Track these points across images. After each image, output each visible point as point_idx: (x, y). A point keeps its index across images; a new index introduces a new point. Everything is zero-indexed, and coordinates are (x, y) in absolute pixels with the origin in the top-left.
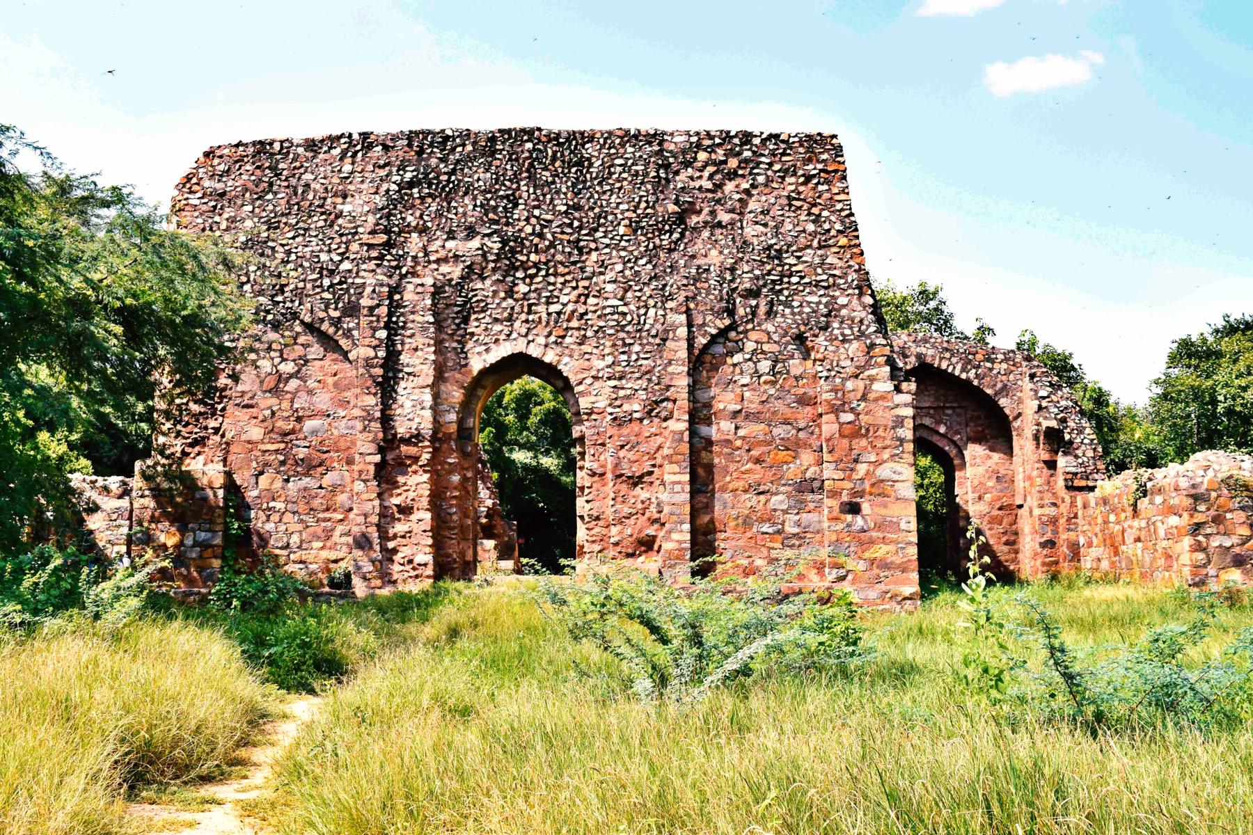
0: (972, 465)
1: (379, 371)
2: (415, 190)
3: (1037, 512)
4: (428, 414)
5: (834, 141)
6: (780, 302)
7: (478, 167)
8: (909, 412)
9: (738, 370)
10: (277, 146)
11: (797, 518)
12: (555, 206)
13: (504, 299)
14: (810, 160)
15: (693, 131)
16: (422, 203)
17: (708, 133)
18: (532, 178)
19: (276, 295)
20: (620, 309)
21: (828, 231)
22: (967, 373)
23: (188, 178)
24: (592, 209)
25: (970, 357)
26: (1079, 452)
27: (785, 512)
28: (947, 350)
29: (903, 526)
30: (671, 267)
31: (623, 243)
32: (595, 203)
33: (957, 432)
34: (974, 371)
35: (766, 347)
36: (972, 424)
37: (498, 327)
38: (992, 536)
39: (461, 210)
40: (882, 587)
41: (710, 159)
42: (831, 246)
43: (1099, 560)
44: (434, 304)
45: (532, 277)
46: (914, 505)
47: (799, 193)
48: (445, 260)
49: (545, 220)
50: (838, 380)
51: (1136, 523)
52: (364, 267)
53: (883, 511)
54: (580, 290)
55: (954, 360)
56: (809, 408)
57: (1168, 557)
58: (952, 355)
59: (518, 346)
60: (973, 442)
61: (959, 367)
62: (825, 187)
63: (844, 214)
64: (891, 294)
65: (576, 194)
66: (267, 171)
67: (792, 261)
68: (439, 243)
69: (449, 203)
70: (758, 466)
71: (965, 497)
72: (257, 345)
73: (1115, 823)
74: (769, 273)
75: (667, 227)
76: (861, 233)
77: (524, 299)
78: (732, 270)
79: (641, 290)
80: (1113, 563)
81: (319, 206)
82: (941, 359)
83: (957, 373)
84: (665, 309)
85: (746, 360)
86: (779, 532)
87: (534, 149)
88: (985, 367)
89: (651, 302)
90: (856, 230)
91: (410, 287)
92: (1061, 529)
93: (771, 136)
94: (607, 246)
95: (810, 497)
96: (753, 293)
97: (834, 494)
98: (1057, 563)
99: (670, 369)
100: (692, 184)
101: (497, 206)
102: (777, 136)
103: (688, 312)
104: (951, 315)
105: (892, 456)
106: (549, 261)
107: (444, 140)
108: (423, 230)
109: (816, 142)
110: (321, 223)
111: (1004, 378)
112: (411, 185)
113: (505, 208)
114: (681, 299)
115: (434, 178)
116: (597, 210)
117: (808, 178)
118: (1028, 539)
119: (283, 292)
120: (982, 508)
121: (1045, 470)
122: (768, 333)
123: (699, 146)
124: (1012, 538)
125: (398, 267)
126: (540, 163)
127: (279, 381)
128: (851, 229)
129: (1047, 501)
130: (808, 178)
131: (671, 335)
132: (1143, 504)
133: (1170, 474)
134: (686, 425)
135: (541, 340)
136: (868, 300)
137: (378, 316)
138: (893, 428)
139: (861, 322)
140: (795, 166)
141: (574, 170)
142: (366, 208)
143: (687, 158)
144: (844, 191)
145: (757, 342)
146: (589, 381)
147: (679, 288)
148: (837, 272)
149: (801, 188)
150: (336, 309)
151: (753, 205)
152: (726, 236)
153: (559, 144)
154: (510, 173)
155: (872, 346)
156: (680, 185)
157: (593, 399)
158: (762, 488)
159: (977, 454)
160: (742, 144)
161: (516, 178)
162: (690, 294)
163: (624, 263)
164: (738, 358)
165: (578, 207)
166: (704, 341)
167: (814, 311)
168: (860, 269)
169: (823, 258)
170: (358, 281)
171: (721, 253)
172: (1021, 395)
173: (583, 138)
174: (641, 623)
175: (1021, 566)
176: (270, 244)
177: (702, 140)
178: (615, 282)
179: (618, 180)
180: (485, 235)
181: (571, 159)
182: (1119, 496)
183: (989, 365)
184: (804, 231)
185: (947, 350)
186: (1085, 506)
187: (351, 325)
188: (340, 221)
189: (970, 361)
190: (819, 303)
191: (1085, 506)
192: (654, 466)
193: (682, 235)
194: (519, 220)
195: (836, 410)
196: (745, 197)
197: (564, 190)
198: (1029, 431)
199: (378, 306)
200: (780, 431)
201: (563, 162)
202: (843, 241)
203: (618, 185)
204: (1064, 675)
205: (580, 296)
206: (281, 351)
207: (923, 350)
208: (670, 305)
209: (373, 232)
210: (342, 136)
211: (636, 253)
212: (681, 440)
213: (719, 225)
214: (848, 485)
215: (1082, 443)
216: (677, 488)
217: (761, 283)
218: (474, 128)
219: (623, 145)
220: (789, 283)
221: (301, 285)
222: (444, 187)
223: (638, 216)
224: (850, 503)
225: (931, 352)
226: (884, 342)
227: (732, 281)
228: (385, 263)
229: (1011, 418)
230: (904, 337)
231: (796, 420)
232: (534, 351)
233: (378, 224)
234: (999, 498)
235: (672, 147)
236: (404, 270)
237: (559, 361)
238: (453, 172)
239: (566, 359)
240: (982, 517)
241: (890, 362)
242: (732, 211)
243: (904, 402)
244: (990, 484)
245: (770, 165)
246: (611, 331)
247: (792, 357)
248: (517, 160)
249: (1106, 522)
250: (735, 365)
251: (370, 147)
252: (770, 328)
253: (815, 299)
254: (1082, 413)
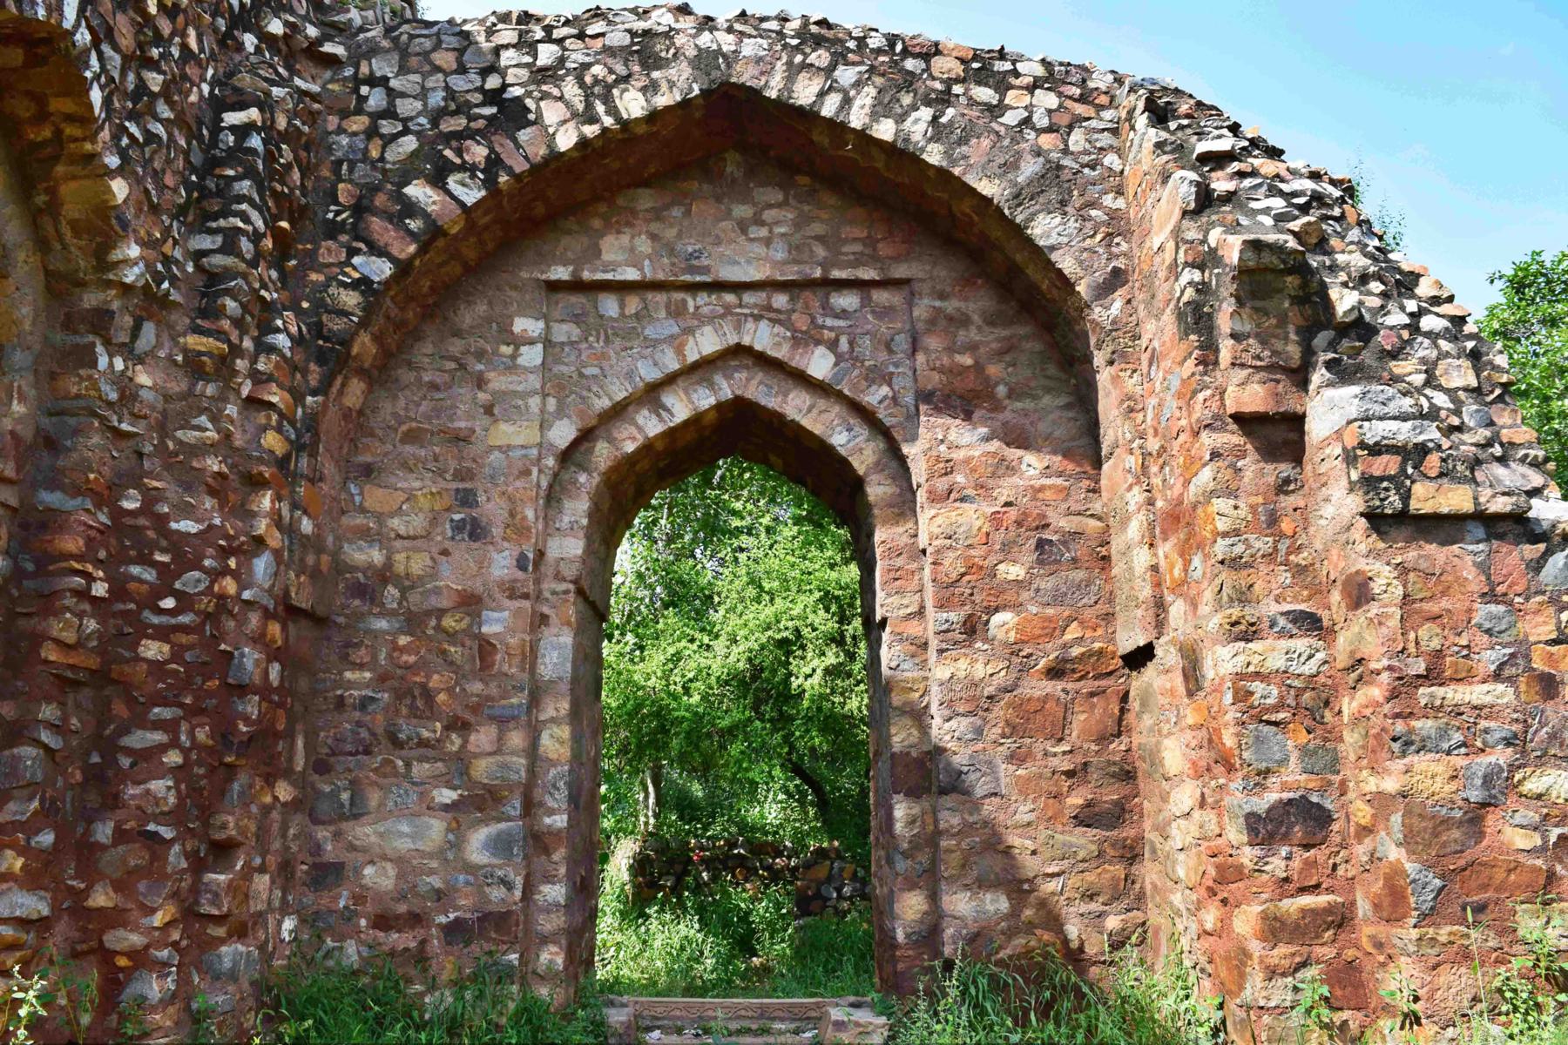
0: (935, 498)
22: (900, 119)
25: (910, 64)
34: (926, 113)
36: (933, 342)
55: (846, 75)
58: (840, 58)
60: (938, 410)
61: (865, 99)
71: (914, 628)
82: (793, 71)
83: (857, 119)
88: (972, 102)
92: (1351, 740)
98: (1340, 919)
111: (1046, 141)
118: (1184, 796)
120: (980, 671)
121: (1250, 464)
124: (1111, 795)
129: (1271, 608)
159: (958, 455)
172: (1120, 203)
175: (1155, 918)
183: (985, 94)
189: (910, 80)
215: (1414, 328)
229: (1081, 288)
234: (1053, 629)
240: (978, 703)
244: (1013, 571)
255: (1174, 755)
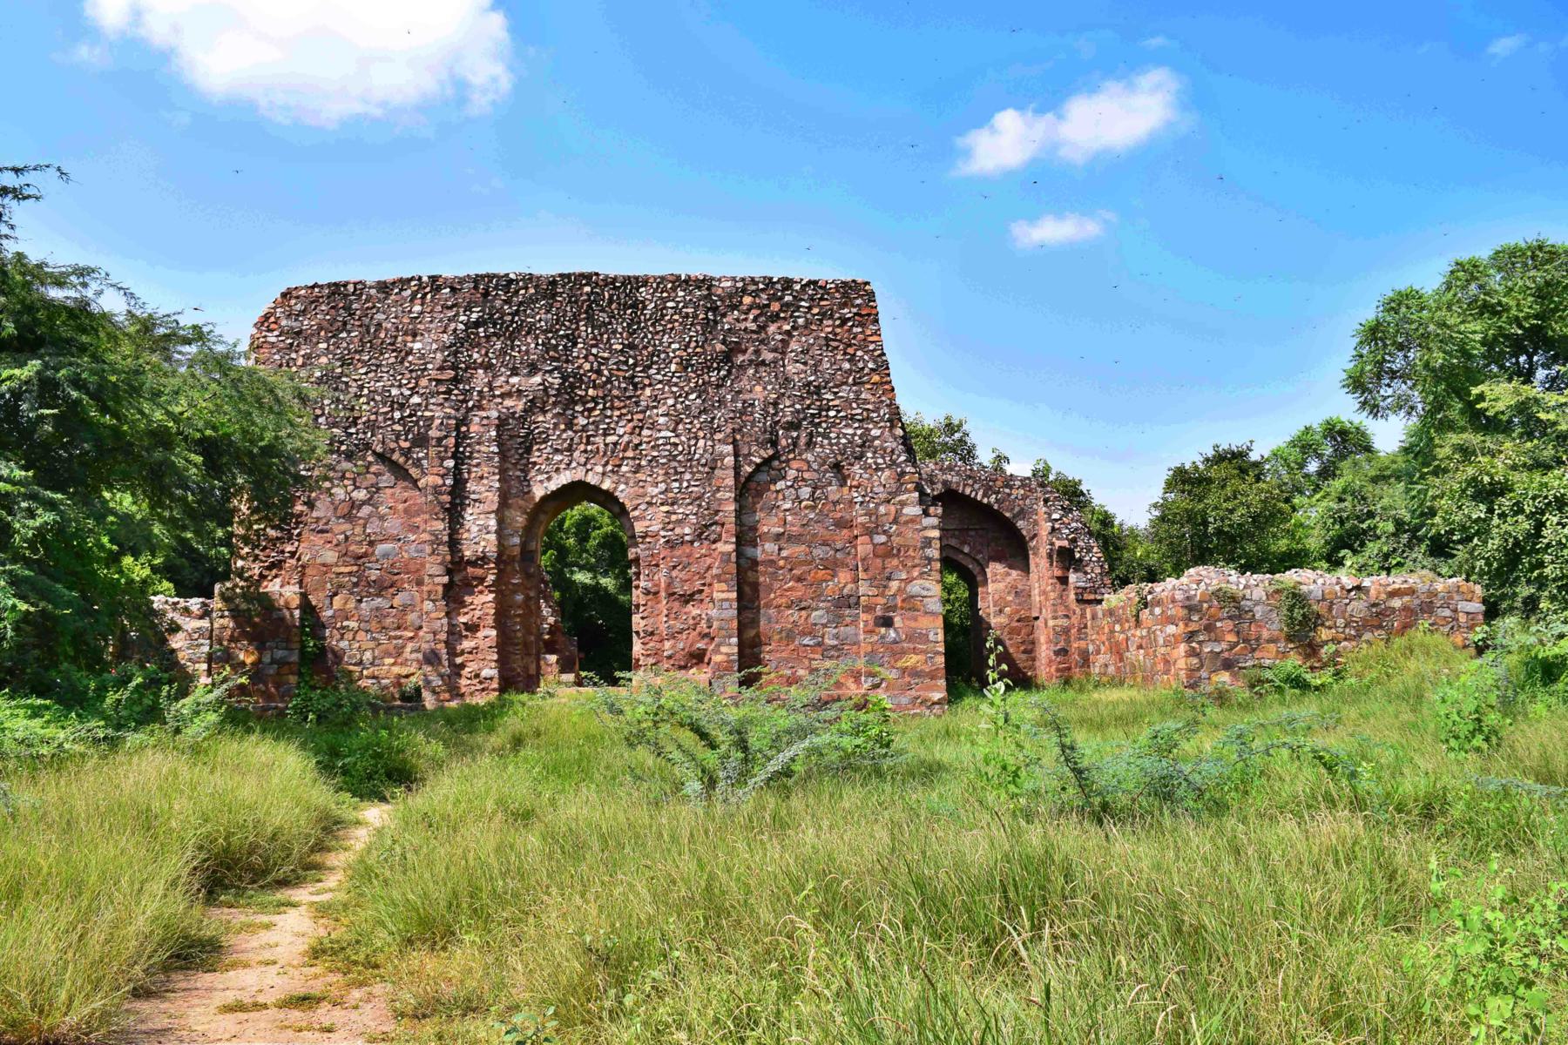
1: (447, 498)
2: (481, 330)
3: (1051, 623)
4: (493, 537)
5: (867, 287)
6: (819, 434)
7: (540, 309)
8: (936, 533)
9: (781, 497)
10: (351, 288)
11: (835, 631)
12: (611, 345)
13: (564, 431)
14: (844, 305)
15: (739, 275)
16: (487, 342)
17: (753, 279)
18: (590, 319)
19: (350, 427)
20: (672, 440)
21: (863, 369)
23: (266, 317)
24: (645, 348)
26: (1088, 569)
27: (825, 626)
28: (970, 477)
29: (931, 637)
30: (719, 401)
31: (674, 380)
32: (649, 342)
33: (980, 552)
35: (806, 475)
37: (558, 457)
38: (1012, 645)
39: (524, 348)
40: (913, 693)
41: (754, 302)
42: (864, 383)
43: (1106, 666)
44: (498, 436)
45: (590, 410)
46: (941, 618)
47: (836, 335)
48: (508, 395)
49: (603, 358)
50: (872, 505)
51: (1138, 633)
52: (432, 401)
53: (913, 624)
54: (635, 423)
55: (976, 486)
56: (845, 531)
57: (1167, 662)
58: (975, 482)
59: (578, 474)
61: (981, 493)
62: (859, 330)
63: (876, 353)
64: (919, 427)
65: (631, 334)
66: (342, 311)
67: (831, 397)
68: (502, 379)
69: (513, 342)
70: (800, 585)
72: (331, 474)
73: (1031, 906)
74: (809, 407)
75: (715, 365)
76: (892, 371)
77: (582, 431)
78: (775, 404)
79: (691, 423)
80: (1119, 668)
81: (390, 344)
82: (965, 485)
83: (979, 498)
84: (713, 440)
85: (788, 487)
86: (819, 644)
87: (592, 292)
89: (701, 434)
90: (888, 368)
91: (477, 420)
93: (810, 282)
94: (660, 382)
95: (847, 612)
96: (793, 426)
97: (869, 609)
98: (1069, 669)
99: (718, 495)
100: (738, 326)
101: (557, 345)
102: (815, 283)
103: (734, 443)
104: (974, 446)
105: (922, 574)
106: (606, 396)
107: (507, 283)
108: (487, 367)
109: (850, 288)
110: (392, 360)
112: (477, 324)
113: (565, 346)
114: (728, 431)
115: (499, 318)
116: (650, 349)
117: (844, 321)
118: (1044, 647)
119: (356, 425)
121: (1058, 586)
122: (808, 462)
123: (744, 291)
124: (1030, 647)
125: (467, 402)
126: (597, 305)
127: (352, 507)
128: (883, 367)
130: (844, 321)
131: (719, 464)
132: (1145, 614)
133: (1168, 586)
134: (733, 546)
135: (599, 469)
136: (899, 432)
137: (446, 447)
138: (923, 548)
139: (893, 451)
140: (831, 310)
141: (629, 311)
142: (435, 346)
143: (733, 299)
144: (877, 333)
145: (798, 470)
146: (643, 507)
147: (726, 421)
148: (870, 407)
149: (838, 330)
150: (406, 440)
151: (794, 345)
152: (769, 374)
153: (616, 288)
154: (569, 314)
155: (903, 473)
156: (726, 327)
157: (648, 523)
158: (803, 604)
160: (784, 289)
161: (575, 319)
162: (736, 426)
163: (676, 398)
164: (780, 485)
165: (632, 346)
166: (749, 470)
167: (850, 442)
168: (891, 404)
169: (858, 393)
170: (427, 414)
171: (765, 388)
173: (637, 282)
174: (692, 730)
176: (344, 379)
177: (747, 286)
178: (667, 415)
179: (670, 321)
180: (547, 372)
181: (626, 303)
182: (1123, 608)
183: (1007, 491)
184: (840, 369)
185: (970, 477)
186: (1094, 617)
187: (421, 455)
188: (410, 358)
190: (855, 434)
191: (1094, 617)
192: (704, 585)
193: (729, 372)
194: (578, 357)
195: (870, 532)
196: (786, 337)
197: (620, 330)
198: (1044, 550)
199: (446, 437)
200: (819, 552)
201: (619, 304)
202: (876, 378)
203: (669, 326)
204: (1073, 770)
205: (634, 428)
206: (354, 480)
207: (949, 477)
208: (718, 436)
209: (441, 369)
210: (412, 279)
211: (686, 389)
212: (729, 561)
213: (763, 363)
214: (884, 601)
216: (726, 605)
217: (802, 416)
218: (536, 272)
219: (674, 289)
220: (827, 416)
221: (373, 417)
222: (508, 327)
223: (689, 354)
224: (883, 617)
225: (955, 479)
226: (913, 470)
227: (775, 414)
228: (453, 397)
230: (932, 466)
231: (834, 541)
232: (592, 479)
233: (445, 361)
234: (1017, 611)
235: (719, 291)
236: (470, 404)
237: (615, 489)
238: (517, 313)
239: (622, 487)
240: (1003, 628)
241: (919, 488)
242: (774, 350)
243: (931, 527)
245: (810, 308)
246: (664, 461)
247: (830, 484)
248: (576, 302)
249: (1112, 631)
250: (778, 492)
251: (439, 289)
252: (809, 457)
253: (850, 431)
254: (1090, 533)
255: (1043, 639)
